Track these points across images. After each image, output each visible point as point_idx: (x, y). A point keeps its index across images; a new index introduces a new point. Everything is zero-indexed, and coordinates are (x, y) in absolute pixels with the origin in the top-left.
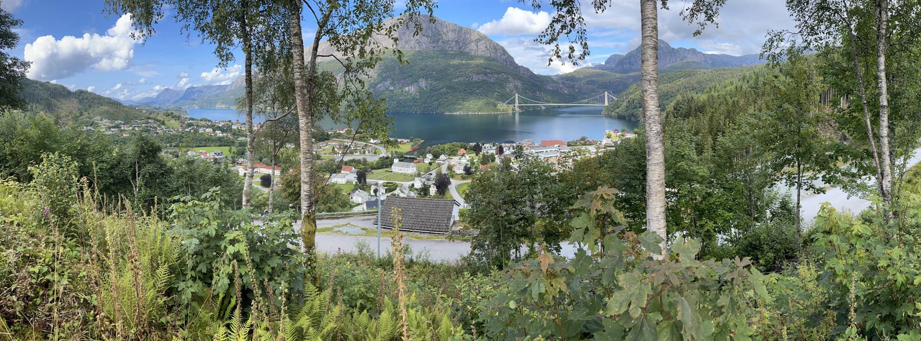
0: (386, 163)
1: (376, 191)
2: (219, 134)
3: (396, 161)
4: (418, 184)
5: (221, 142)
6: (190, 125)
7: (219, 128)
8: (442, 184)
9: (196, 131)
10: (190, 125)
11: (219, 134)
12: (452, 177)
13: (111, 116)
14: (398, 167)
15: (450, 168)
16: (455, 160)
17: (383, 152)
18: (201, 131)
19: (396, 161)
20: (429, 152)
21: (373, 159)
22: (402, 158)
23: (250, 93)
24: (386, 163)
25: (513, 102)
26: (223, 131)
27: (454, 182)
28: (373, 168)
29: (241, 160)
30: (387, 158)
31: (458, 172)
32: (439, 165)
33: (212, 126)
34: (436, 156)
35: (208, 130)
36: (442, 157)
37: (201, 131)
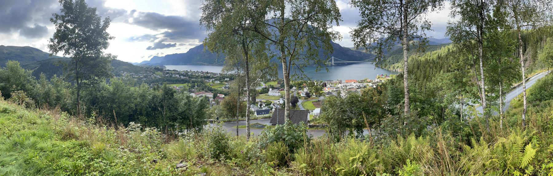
0: (265, 91)
1: (261, 105)
2: (182, 77)
3: (271, 89)
4: (281, 102)
5: (183, 81)
6: (168, 73)
7: (182, 75)
8: (294, 102)
9: (171, 77)
10: (168, 73)
11: (182, 77)
12: (300, 98)
13: (127, 70)
14: (271, 92)
15: (298, 93)
17: (263, 85)
18: (173, 76)
19: (271, 89)
22: (273, 88)
23: (247, 64)
24: (265, 91)
25: (331, 61)
26: (184, 76)
27: (300, 101)
29: (193, 90)
30: (266, 88)
31: (302, 95)
32: (293, 92)
33: (178, 74)
35: (177, 75)
37: (173, 76)
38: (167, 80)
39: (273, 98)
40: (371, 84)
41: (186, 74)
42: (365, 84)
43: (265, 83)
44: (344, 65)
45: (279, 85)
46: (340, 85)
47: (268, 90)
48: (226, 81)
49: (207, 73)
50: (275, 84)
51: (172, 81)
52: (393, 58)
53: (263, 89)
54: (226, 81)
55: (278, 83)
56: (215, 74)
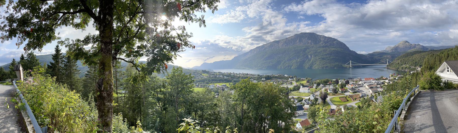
0: (297, 89)
14: (302, 90)
16: (327, 87)
17: (295, 84)
19: (301, 87)
20: (315, 83)
21: (291, 87)
22: (304, 86)
28: (291, 91)
34: (318, 85)
36: (321, 85)
38: (213, 80)
39: (304, 95)
40: (387, 81)
41: (229, 75)
42: (382, 81)
43: (297, 81)
44: (359, 67)
45: (308, 84)
46: (361, 82)
47: (299, 88)
48: (263, 81)
49: (247, 74)
50: (304, 82)
51: (216, 81)
52: (401, 60)
53: (295, 86)
54: (263, 81)
55: (308, 82)
56: (254, 75)
